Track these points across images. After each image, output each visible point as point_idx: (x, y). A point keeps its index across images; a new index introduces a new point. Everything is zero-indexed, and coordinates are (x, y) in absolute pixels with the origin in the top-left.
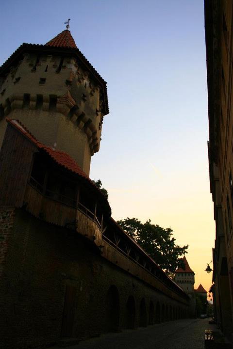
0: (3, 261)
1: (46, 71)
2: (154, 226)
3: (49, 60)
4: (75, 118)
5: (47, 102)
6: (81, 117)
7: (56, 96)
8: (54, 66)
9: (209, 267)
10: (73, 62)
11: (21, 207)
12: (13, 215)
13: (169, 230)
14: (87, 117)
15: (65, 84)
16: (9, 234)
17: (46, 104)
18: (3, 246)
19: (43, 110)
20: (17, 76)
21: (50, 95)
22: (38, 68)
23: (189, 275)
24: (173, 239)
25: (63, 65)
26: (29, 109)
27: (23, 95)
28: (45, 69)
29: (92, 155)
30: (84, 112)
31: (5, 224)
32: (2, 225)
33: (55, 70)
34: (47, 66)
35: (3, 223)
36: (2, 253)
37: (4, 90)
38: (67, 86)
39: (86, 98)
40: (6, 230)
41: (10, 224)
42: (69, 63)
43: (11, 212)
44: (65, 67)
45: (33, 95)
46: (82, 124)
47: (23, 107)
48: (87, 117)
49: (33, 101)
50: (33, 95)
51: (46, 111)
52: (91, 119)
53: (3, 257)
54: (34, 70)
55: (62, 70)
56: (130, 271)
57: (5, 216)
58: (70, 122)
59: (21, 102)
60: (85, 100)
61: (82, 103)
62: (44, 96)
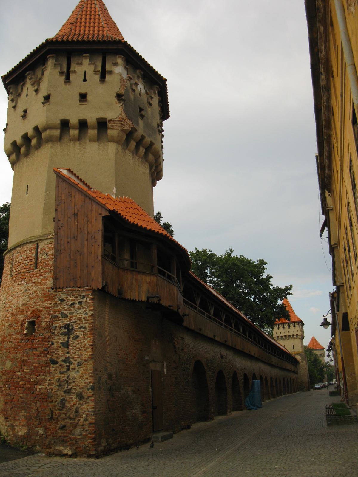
0: (89, 355)
1: (85, 80)
2: (234, 257)
3: (86, 62)
4: (133, 144)
5: (93, 128)
6: (140, 142)
7: (106, 119)
8: (96, 72)
9: (325, 319)
10: (120, 61)
11: (100, 288)
12: (92, 299)
13: (262, 263)
14: (148, 140)
15: (116, 100)
16: (92, 323)
17: (92, 132)
18: (86, 337)
19: (90, 141)
20: (43, 92)
21: (97, 119)
22: (72, 77)
23: (295, 326)
24: (269, 277)
25: (108, 68)
26: (70, 140)
27: (59, 122)
28: (83, 77)
29: (154, 184)
30: (144, 134)
31: (83, 310)
32: (80, 311)
33: (98, 77)
34: (85, 72)
35: (80, 309)
36: (87, 345)
37: (25, 111)
38: (120, 103)
39: (143, 113)
40: (86, 318)
41: (90, 310)
42: (116, 64)
43: (88, 295)
45: (74, 121)
46: (142, 150)
47: (60, 139)
48: (148, 140)
49: (74, 128)
50: (74, 121)
51: (94, 141)
52: (153, 141)
53: (90, 350)
54: (68, 79)
55: (107, 77)
56: (216, 338)
57: (81, 300)
58: (127, 152)
59: (57, 132)
60: (142, 116)
61: (141, 122)
62: (88, 121)
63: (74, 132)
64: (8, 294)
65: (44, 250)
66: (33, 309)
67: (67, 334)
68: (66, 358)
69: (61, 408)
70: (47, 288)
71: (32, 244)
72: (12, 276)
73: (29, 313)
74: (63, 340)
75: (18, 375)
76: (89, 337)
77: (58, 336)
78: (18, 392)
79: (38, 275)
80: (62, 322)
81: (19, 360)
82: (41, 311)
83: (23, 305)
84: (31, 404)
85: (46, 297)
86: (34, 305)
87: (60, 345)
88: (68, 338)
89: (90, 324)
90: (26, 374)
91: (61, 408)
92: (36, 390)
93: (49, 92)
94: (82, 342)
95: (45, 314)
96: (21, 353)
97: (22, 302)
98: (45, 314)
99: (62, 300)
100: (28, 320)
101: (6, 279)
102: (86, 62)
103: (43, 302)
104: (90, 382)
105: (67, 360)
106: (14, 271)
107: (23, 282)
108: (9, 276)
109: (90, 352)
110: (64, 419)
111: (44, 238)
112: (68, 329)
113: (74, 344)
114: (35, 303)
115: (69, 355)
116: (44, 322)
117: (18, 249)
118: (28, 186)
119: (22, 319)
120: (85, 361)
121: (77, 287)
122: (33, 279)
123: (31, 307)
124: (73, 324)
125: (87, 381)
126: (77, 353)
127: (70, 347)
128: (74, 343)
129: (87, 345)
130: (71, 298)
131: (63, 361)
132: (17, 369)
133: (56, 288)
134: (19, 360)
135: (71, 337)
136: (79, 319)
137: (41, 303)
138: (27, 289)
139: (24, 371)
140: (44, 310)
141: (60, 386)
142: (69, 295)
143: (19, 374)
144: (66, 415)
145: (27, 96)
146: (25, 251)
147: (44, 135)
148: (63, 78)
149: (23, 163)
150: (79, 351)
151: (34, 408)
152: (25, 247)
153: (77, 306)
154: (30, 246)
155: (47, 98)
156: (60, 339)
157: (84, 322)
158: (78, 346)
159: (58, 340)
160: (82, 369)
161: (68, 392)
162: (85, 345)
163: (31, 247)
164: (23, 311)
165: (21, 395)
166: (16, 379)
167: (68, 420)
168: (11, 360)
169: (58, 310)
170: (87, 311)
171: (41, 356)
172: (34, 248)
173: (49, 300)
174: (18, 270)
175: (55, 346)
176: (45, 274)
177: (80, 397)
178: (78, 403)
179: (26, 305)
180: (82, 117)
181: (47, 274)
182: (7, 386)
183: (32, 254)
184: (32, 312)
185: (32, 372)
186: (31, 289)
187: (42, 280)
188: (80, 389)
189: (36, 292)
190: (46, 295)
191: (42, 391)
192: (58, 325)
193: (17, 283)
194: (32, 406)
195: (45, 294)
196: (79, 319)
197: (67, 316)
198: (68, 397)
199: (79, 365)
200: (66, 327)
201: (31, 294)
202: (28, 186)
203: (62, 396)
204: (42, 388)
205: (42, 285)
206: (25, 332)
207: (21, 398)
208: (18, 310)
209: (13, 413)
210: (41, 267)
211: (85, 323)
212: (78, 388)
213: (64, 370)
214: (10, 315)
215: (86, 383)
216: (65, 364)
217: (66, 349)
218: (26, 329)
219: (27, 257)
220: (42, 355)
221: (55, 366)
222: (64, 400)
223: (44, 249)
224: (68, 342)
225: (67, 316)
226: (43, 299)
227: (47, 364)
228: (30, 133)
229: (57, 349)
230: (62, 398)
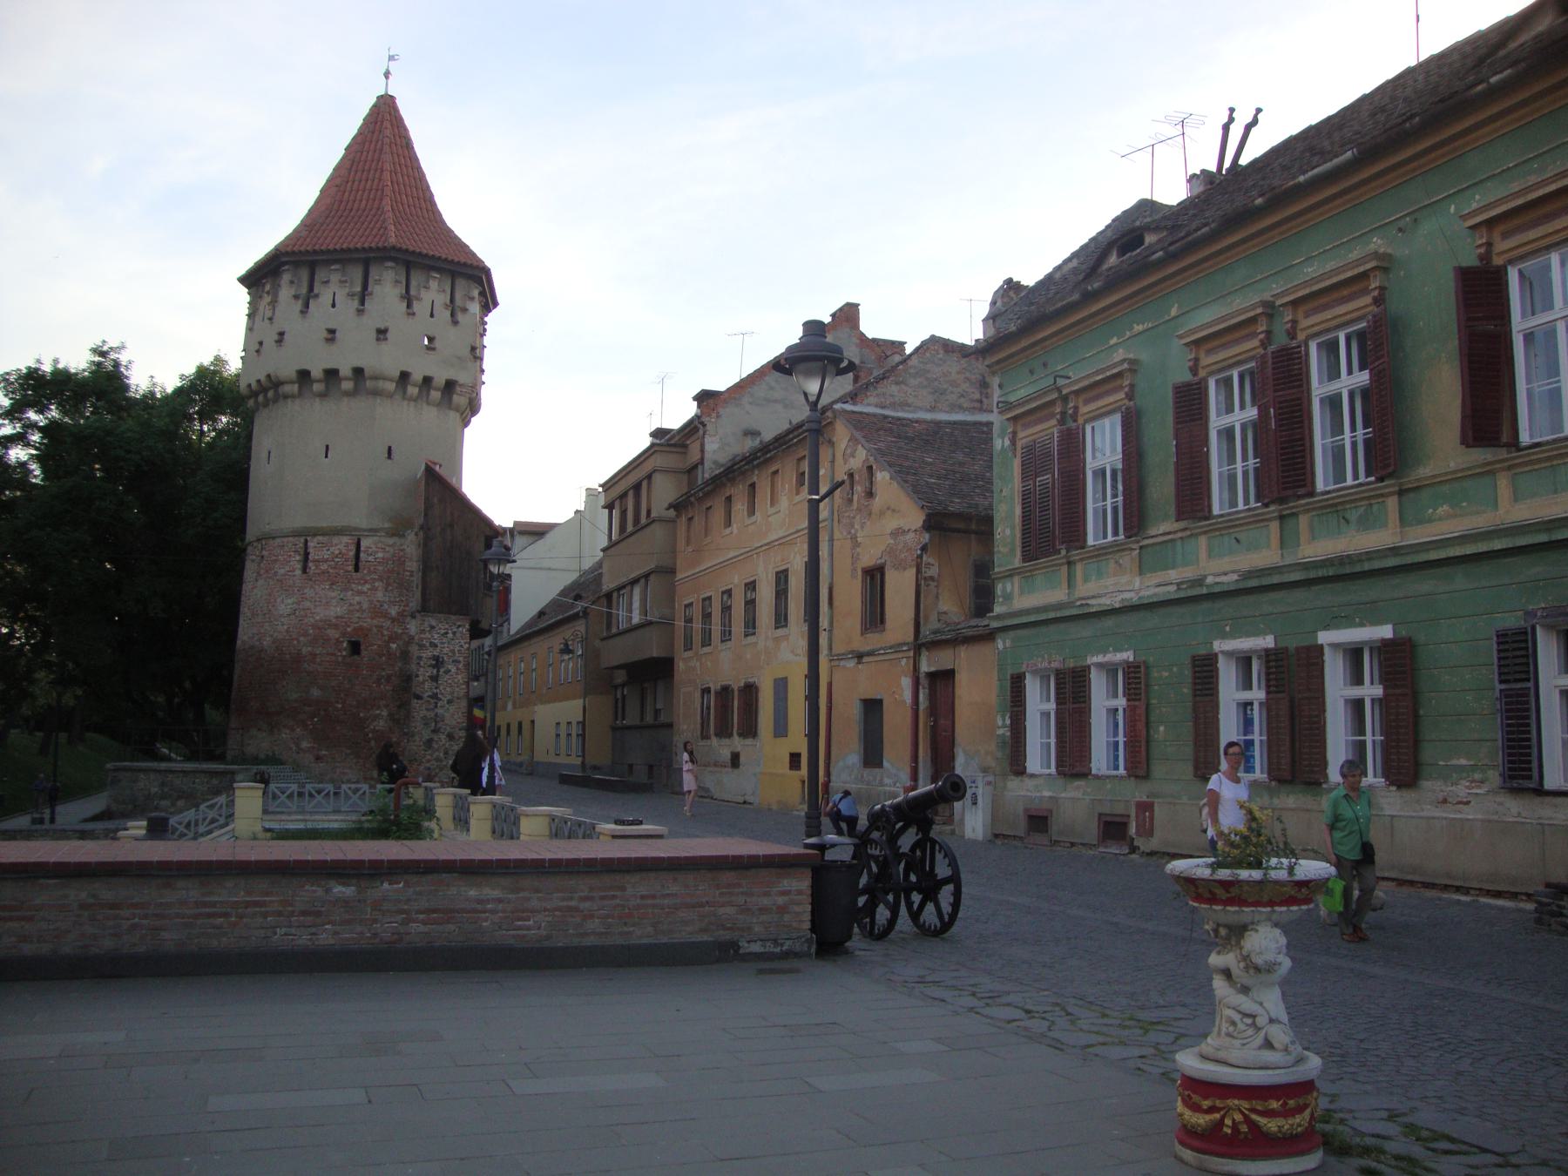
3: (434, 284)
22: (416, 306)
26: (404, 398)
33: (448, 313)
37: (332, 332)
44: (465, 310)
50: (417, 376)
55: (460, 317)
59: (391, 386)
63: (413, 391)
72: (305, 570)
78: (338, 728)
82: (370, 630)
83: (337, 617)
88: (438, 671)
93: (387, 324)
99: (432, 627)
102: (434, 284)
103: (372, 619)
105: (435, 696)
108: (298, 572)
110: (429, 761)
112: (438, 662)
117: (320, 538)
118: (327, 447)
119: (337, 636)
120: (458, 698)
122: (353, 586)
128: (444, 679)
131: (429, 696)
135: (442, 670)
136: (453, 651)
137: (369, 620)
140: (375, 630)
141: (425, 724)
143: (340, 706)
144: (431, 755)
145: (334, 306)
146: (336, 545)
147: (369, 384)
148: (405, 304)
152: (335, 540)
153: (450, 635)
154: (345, 539)
155: (382, 333)
159: (424, 673)
167: (434, 762)
175: (421, 678)
177: (451, 737)
180: (428, 373)
181: (377, 584)
183: (351, 550)
184: (355, 629)
189: (359, 603)
192: (424, 655)
197: (436, 646)
199: (449, 702)
200: (436, 658)
201: (351, 605)
202: (327, 447)
206: (344, 653)
212: (448, 728)
213: (432, 707)
216: (432, 701)
218: (345, 649)
221: (419, 701)
222: (430, 741)
224: (438, 676)
225: (436, 646)
228: (345, 371)
229: (423, 683)
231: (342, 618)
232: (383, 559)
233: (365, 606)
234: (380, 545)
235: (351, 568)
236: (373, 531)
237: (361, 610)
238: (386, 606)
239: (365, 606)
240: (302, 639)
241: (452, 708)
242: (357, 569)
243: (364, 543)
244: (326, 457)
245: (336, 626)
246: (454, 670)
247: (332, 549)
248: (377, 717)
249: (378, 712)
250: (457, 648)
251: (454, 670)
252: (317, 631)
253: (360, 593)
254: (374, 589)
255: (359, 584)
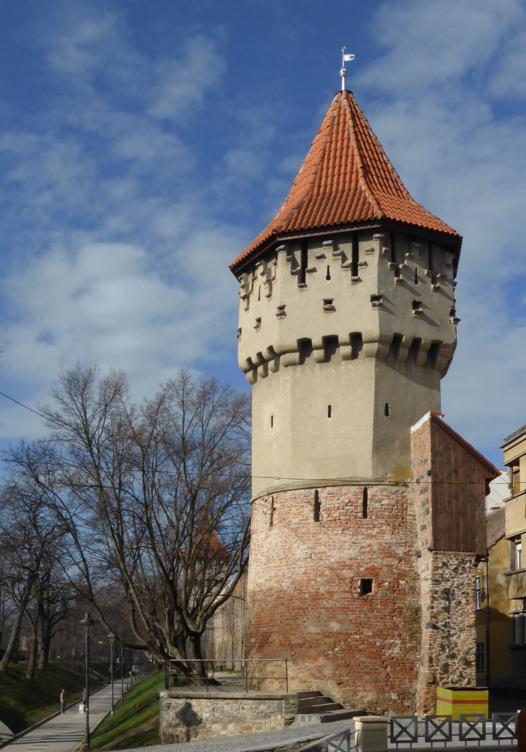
32: (461, 576)
36: (470, 611)
40: (469, 584)
53: (473, 616)
64: (316, 543)
65: (377, 498)
66: (368, 565)
67: (448, 599)
68: (446, 623)
69: (443, 672)
70: (386, 543)
71: (357, 487)
72: (317, 518)
73: (362, 569)
74: (445, 604)
75: (355, 638)
76: (472, 603)
77: (438, 600)
78: (357, 656)
79: (371, 526)
80: (442, 586)
81: (354, 621)
83: (351, 559)
84: (378, 669)
85: (386, 553)
86: (369, 561)
87: (440, 609)
88: (450, 603)
89: (472, 590)
90: (367, 637)
91: (443, 672)
92: (384, 655)
94: (464, 608)
95: (387, 572)
96: (355, 614)
97: (349, 555)
98: (387, 572)
99: (444, 564)
100: (362, 578)
101: (301, 522)
103: (383, 559)
104: (473, 648)
106: (326, 516)
107: (346, 532)
108: (312, 520)
109: (473, 618)
111: (377, 483)
113: (457, 610)
114: (371, 559)
115: (450, 620)
116: (386, 582)
118: (330, 407)
119: (352, 576)
121: (459, 551)
122: (363, 530)
123: (364, 563)
124: (454, 588)
125: (470, 646)
126: (459, 619)
127: (451, 612)
129: (470, 611)
130: (453, 562)
131: (442, 626)
132: (353, 632)
133: (436, 550)
134: (354, 621)
137: (380, 560)
138: (356, 542)
139: (364, 633)
140: (385, 569)
142: (451, 559)
143: (358, 637)
146: (345, 494)
149: (312, 371)
150: (461, 616)
151: (384, 673)
152: (344, 489)
156: (441, 604)
157: (466, 588)
158: (460, 612)
160: (465, 634)
161: (453, 656)
162: (468, 611)
163: (356, 490)
164: (352, 566)
165: (362, 659)
166: (354, 643)
168: (340, 622)
169: (438, 574)
170: (470, 577)
171: (386, 618)
172: (360, 492)
173: (390, 557)
174: (334, 515)
176: (381, 527)
178: (460, 668)
179: (357, 559)
181: (384, 528)
182: (336, 649)
183: (359, 499)
184: (367, 569)
185: (374, 636)
186: (362, 542)
187: (378, 533)
188: (463, 654)
189: (369, 546)
190: (386, 551)
191: (393, 655)
193: (335, 532)
194: (380, 671)
195: (383, 550)
196: (462, 584)
198: (450, 662)
202: (330, 407)
203: (443, 661)
204: (392, 653)
205: (378, 539)
207: (364, 662)
208: (343, 564)
209: (352, 678)
210: (373, 517)
211: (467, 589)
213: (446, 635)
214: (326, 569)
215: (468, 648)
217: (447, 614)
219: (350, 502)
220: (388, 617)
223: (376, 496)
226: (383, 555)
227: (396, 628)
230: (443, 663)
231: (357, 559)
232: (388, 505)
233: (375, 548)
234: (385, 493)
235: (360, 514)
236: (378, 482)
237: (372, 552)
238: (394, 547)
239: (375, 548)
240: (319, 579)
241: (463, 636)
242: (365, 516)
243: (370, 492)
244: (329, 416)
245: (350, 567)
246: (464, 601)
247: (341, 499)
248: (391, 646)
249: (393, 641)
250: (466, 581)
251: (464, 601)
252: (332, 572)
253: (370, 536)
254: (383, 532)
255: (367, 529)
